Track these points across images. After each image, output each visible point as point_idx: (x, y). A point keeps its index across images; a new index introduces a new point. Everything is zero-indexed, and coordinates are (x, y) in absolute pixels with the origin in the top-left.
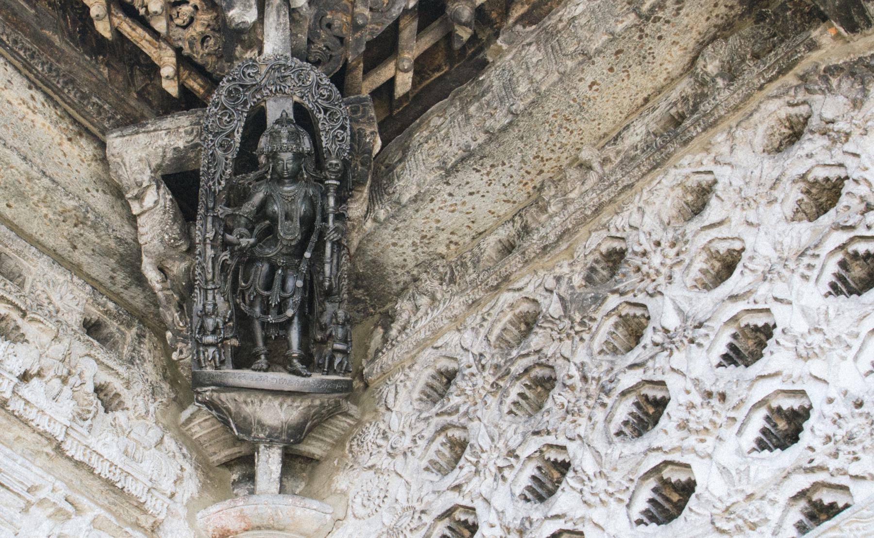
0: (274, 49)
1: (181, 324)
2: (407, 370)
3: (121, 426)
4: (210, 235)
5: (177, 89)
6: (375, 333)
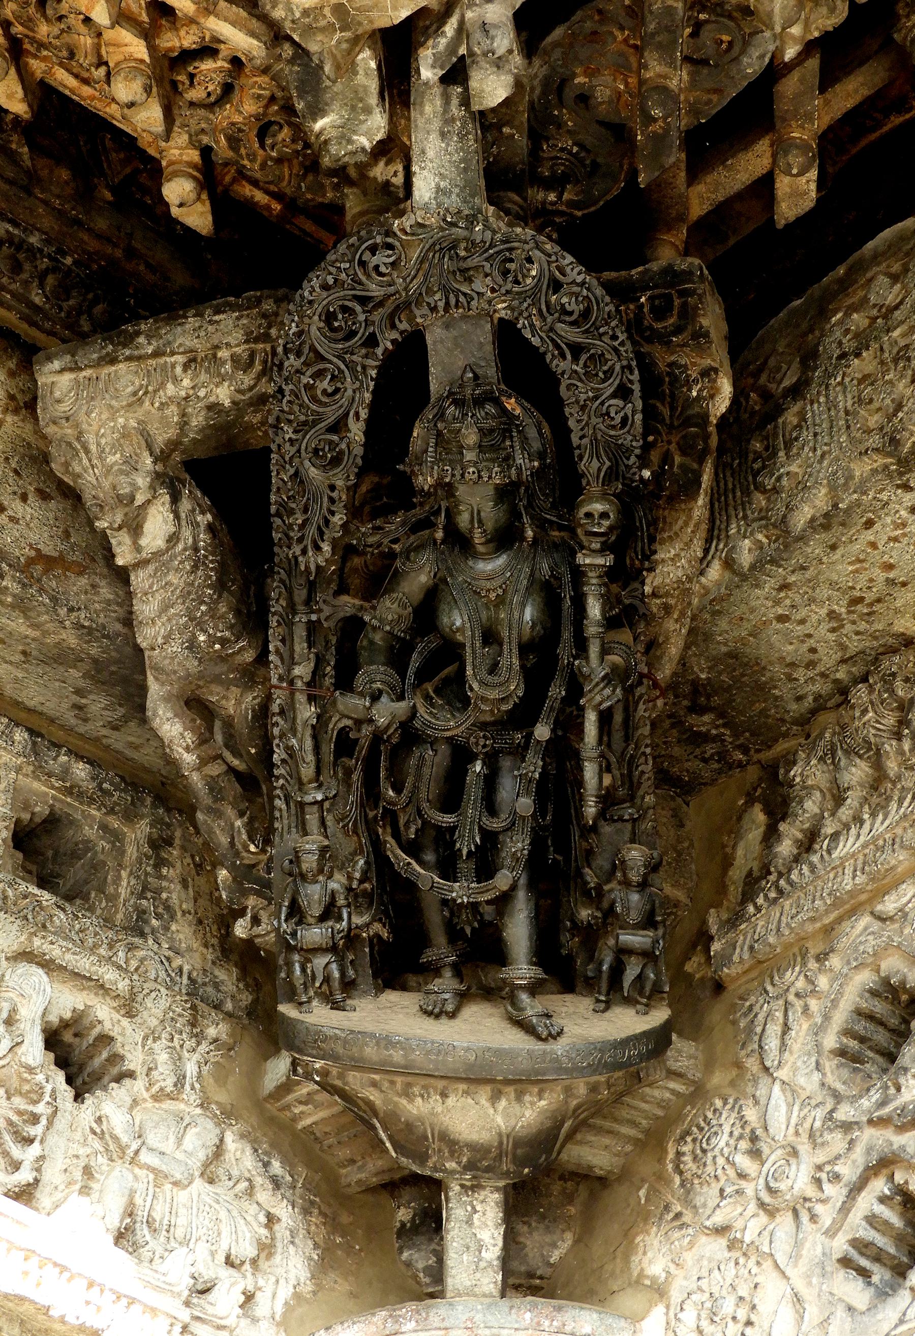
0: (438, 189)
1: (252, 848)
2: (813, 965)
3: (115, 1139)
4: (303, 671)
5: (210, 218)
6: (746, 817)
